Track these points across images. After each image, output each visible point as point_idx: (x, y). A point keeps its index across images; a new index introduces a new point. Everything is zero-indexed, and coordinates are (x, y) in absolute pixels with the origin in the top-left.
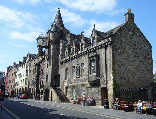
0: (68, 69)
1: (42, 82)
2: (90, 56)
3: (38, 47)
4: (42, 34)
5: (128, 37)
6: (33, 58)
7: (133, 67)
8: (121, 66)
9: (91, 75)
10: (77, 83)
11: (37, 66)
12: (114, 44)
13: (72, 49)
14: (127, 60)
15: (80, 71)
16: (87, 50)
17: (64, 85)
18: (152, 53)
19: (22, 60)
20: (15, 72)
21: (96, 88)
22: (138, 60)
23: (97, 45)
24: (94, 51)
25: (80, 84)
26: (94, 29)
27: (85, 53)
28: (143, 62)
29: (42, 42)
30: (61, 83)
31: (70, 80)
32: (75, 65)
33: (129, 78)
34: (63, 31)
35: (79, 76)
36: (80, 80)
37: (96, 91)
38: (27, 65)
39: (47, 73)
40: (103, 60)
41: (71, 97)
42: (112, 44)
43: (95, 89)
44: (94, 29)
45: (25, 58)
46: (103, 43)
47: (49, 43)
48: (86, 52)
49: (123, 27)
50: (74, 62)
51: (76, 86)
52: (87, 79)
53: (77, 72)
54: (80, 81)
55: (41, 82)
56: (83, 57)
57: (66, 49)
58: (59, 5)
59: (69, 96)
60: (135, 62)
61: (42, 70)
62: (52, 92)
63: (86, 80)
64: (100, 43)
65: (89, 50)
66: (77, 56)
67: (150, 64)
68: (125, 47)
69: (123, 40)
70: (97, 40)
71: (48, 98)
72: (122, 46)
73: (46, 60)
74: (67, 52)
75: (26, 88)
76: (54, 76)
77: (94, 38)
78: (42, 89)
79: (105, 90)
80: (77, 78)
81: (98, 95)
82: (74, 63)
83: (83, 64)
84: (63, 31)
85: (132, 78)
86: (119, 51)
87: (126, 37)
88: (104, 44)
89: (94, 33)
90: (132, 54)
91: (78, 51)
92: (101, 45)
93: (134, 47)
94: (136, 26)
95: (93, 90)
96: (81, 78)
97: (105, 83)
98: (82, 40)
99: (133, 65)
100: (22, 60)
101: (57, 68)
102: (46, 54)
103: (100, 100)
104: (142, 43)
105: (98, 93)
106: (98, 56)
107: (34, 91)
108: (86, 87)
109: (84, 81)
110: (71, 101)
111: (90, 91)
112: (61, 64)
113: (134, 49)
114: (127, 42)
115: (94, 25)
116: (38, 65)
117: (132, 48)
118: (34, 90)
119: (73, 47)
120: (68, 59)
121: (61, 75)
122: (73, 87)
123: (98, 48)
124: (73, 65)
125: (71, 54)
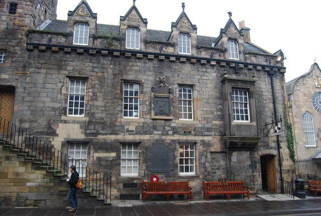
10: (156, 137)
17: (54, 134)
21: (246, 155)
25: (173, 141)
37: (244, 162)
63: (206, 133)
81: (253, 172)
97: (274, 145)
109: (195, 135)
121: (19, 90)
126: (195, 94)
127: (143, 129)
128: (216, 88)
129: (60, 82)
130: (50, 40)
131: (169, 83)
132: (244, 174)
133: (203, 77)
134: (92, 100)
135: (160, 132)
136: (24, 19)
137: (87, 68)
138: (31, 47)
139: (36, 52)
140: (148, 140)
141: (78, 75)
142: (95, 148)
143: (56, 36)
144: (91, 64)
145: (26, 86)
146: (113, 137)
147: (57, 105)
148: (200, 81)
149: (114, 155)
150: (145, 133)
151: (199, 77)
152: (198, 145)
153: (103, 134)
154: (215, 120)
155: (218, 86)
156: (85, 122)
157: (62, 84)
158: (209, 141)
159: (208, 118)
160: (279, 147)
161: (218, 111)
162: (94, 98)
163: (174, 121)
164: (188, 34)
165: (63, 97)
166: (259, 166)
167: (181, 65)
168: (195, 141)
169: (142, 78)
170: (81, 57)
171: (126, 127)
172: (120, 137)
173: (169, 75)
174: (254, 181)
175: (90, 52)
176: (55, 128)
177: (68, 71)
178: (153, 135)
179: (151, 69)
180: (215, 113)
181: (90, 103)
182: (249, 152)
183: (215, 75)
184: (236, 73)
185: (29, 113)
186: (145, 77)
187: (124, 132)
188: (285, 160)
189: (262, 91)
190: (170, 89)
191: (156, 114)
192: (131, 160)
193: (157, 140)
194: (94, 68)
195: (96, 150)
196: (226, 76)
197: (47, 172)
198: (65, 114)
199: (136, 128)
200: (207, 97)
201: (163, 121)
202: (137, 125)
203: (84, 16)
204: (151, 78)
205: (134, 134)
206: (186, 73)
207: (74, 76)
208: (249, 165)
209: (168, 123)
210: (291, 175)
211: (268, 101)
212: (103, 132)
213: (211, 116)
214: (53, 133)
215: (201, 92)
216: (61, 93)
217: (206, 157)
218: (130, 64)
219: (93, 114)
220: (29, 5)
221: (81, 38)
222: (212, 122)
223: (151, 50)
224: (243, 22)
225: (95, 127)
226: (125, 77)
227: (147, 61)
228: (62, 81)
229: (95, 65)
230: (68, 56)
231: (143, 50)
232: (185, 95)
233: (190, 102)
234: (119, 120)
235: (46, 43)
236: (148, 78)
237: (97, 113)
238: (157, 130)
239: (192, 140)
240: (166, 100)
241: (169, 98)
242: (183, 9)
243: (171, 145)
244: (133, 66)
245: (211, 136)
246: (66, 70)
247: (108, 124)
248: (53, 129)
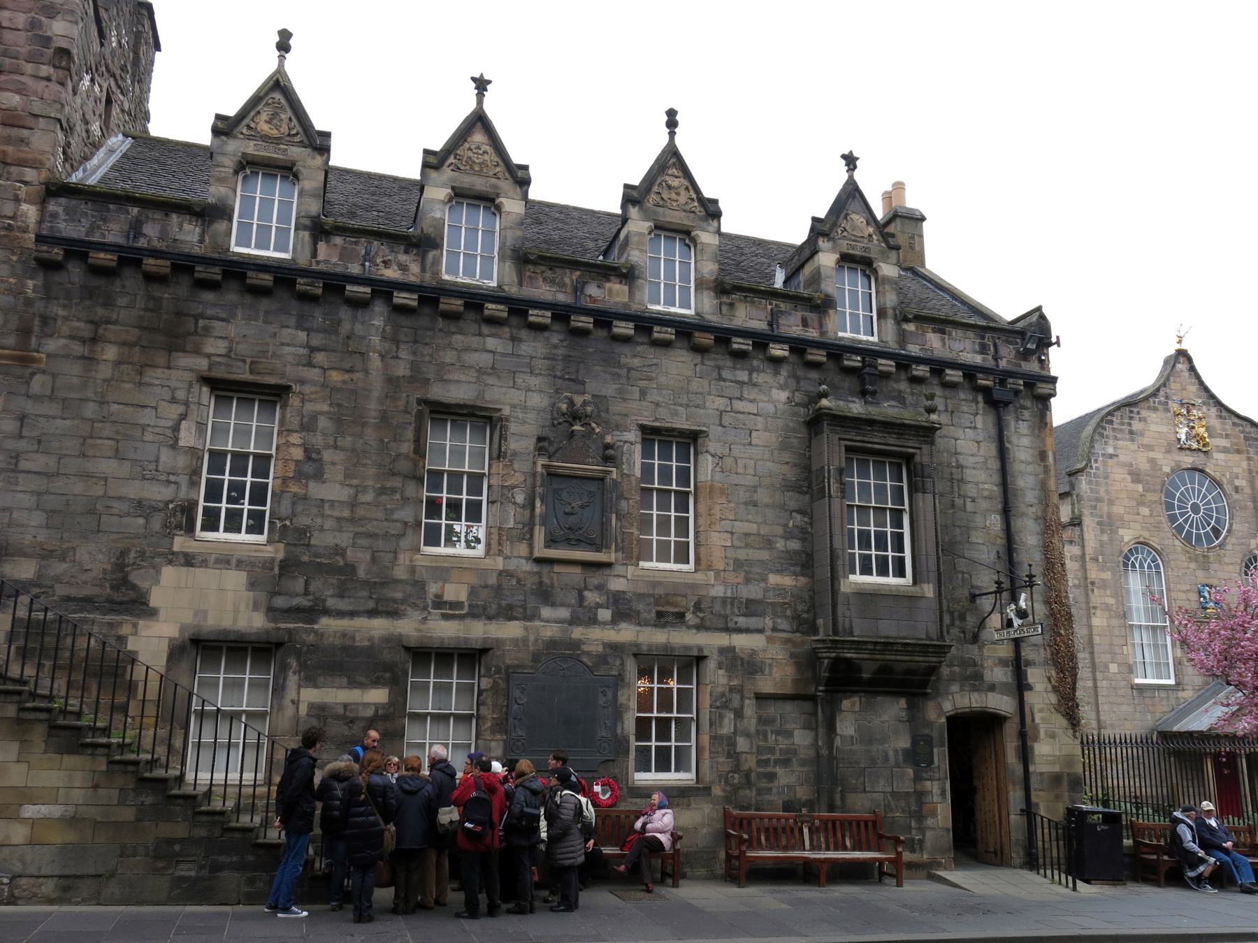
10: (550, 631)
17: (137, 605)
21: (892, 710)
25: (616, 649)
63: (742, 621)
81: (918, 779)
95: (846, 726)
97: (1000, 675)
109: (700, 627)
126: (706, 469)
127: (494, 600)
128: (784, 447)
129: (173, 400)
130: (136, 228)
131: (607, 422)
132: (882, 785)
133: (738, 405)
134: (300, 476)
135: (564, 613)
136: (25, 133)
137: (287, 350)
138: (57, 253)
139: (75, 272)
140: (515, 641)
141: (247, 376)
142: (303, 666)
143: (158, 215)
144: (302, 335)
145: (30, 407)
146: (379, 627)
147: (157, 493)
148: (727, 419)
149: (378, 696)
150: (508, 614)
151: (720, 403)
152: (711, 665)
153: (341, 614)
154: (778, 572)
155: (795, 442)
156: (268, 564)
157: (181, 409)
158: (754, 652)
159: (750, 563)
160: (1021, 686)
161: (788, 536)
162: (309, 468)
163: (619, 569)
164: (688, 233)
165: (182, 461)
166: (941, 756)
167: (652, 354)
168: (700, 649)
169: (501, 396)
170: (265, 304)
171: (433, 589)
172: (408, 627)
173: (609, 389)
174: (920, 817)
175: (302, 284)
176: (143, 584)
177: (209, 356)
178: (537, 623)
179: (540, 364)
180: (780, 545)
181: (294, 488)
182: (903, 702)
183: (783, 396)
184: (863, 394)
185: (37, 518)
186: (516, 396)
187: (425, 608)
188: (1042, 735)
189: (960, 467)
190: (608, 447)
191: (551, 542)
192: (445, 718)
193: (552, 644)
194: (313, 350)
195: (310, 679)
196: (825, 402)
197: (111, 763)
198: (190, 529)
199: (473, 592)
200: (749, 480)
201: (578, 570)
202: (474, 580)
203: (277, 141)
204: (536, 400)
205: (461, 617)
206: (673, 386)
207: (234, 377)
208: (905, 751)
209: (595, 580)
210: (1066, 794)
211: (984, 505)
212: (343, 605)
213: (764, 555)
214: (133, 602)
215: (729, 461)
216: (174, 446)
217: (739, 714)
218: (458, 339)
219: (303, 532)
220: (48, 79)
221: (264, 230)
222: (765, 580)
223: (543, 291)
225: (307, 583)
226: (437, 392)
227: (524, 333)
228: (181, 395)
229: (316, 341)
230: (209, 296)
231: (513, 290)
232: (665, 474)
233: (682, 498)
234: (404, 558)
235: (121, 240)
236: (526, 402)
237: (322, 529)
238: (553, 605)
239: (686, 648)
240: (593, 487)
241: (602, 479)
242: (672, 134)
243: (606, 663)
244: (467, 349)
245: (761, 631)
246: (197, 352)
247: (361, 573)
248: (134, 587)
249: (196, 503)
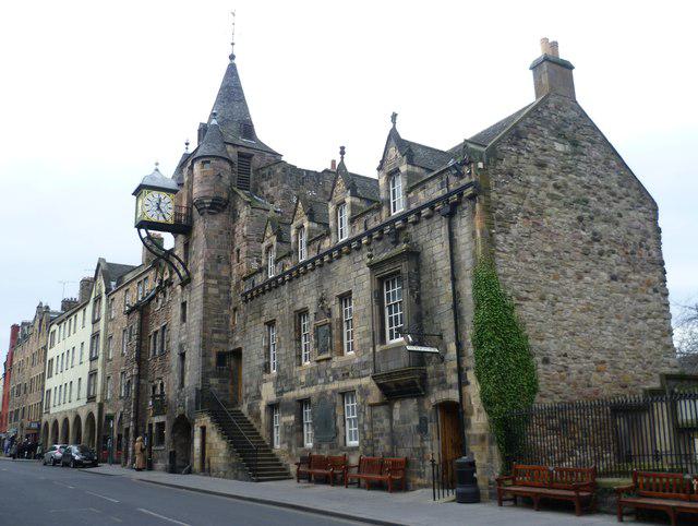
0: (278, 323)
1: (162, 385)
2: (376, 259)
3: (141, 225)
4: (157, 170)
5: (553, 164)
6: (120, 280)
7: (581, 301)
8: (526, 299)
9: (384, 347)
10: (320, 388)
11: (137, 316)
12: (489, 197)
13: (293, 232)
14: (553, 271)
15: (334, 332)
16: (362, 231)
17: (259, 397)
18: (659, 238)
19: (74, 293)
20: (45, 348)
21: (412, 404)
22: (602, 269)
23: (409, 202)
24: (397, 235)
25: (334, 391)
26: (394, 136)
27: (354, 245)
28: (623, 281)
29: (159, 208)
30: (245, 391)
31: (288, 371)
32: (310, 302)
33: (565, 355)
34: (250, 157)
35: (328, 355)
36: (334, 371)
38: (94, 316)
39: (181, 346)
40: (439, 274)
41: (294, 451)
42: (482, 197)
43: (405, 410)
44: (394, 136)
45: (87, 285)
46: (440, 194)
47: (189, 209)
48: (359, 239)
49: (529, 120)
50: (303, 289)
51: (314, 400)
52: (365, 365)
53: (316, 337)
54: (336, 378)
55: (154, 388)
56: (343, 265)
57: (268, 234)
58: (233, 44)
59: (286, 446)
60: (587, 278)
61: (160, 333)
62: (203, 429)
64: (422, 197)
65: (374, 230)
66: (318, 262)
67: (656, 291)
68: (541, 212)
69: (533, 179)
70: (408, 182)
71: (188, 460)
72: (526, 206)
73: (179, 287)
74: (269, 248)
75: (91, 415)
76: (213, 360)
77: (392, 175)
78: (160, 419)
79: (453, 413)
80: (318, 361)
81: (422, 440)
82: (306, 295)
83: (345, 298)
84: (250, 157)
85: (579, 353)
86: (514, 230)
87: (542, 165)
88: (445, 198)
89: (393, 152)
90: (575, 245)
91: (322, 237)
92: (431, 205)
93: (579, 213)
94: (584, 115)
95: (397, 416)
96: (336, 362)
97: (453, 379)
98: (338, 189)
99: (580, 296)
100: (74, 293)
101: (228, 322)
102: (176, 261)
103: (433, 465)
104: (613, 194)
105: (422, 429)
106: (414, 254)
107: (127, 430)
108: (363, 403)
109: (353, 378)
110: (293, 469)
111: (381, 421)
112: (246, 301)
113: (580, 219)
114: (551, 190)
115: (394, 116)
116: (142, 310)
117: (573, 215)
118: (125, 426)
119: (296, 223)
120: (275, 279)
121: (243, 351)
122: (304, 402)
123: (415, 216)
124: (299, 306)
125: (289, 255)
140: (315, 394)
151: (354, 274)
160: (462, 383)
188: (475, 411)
189: (435, 262)
204: (315, 298)
224: (554, 45)
242: (342, 158)
249: (269, 363)
